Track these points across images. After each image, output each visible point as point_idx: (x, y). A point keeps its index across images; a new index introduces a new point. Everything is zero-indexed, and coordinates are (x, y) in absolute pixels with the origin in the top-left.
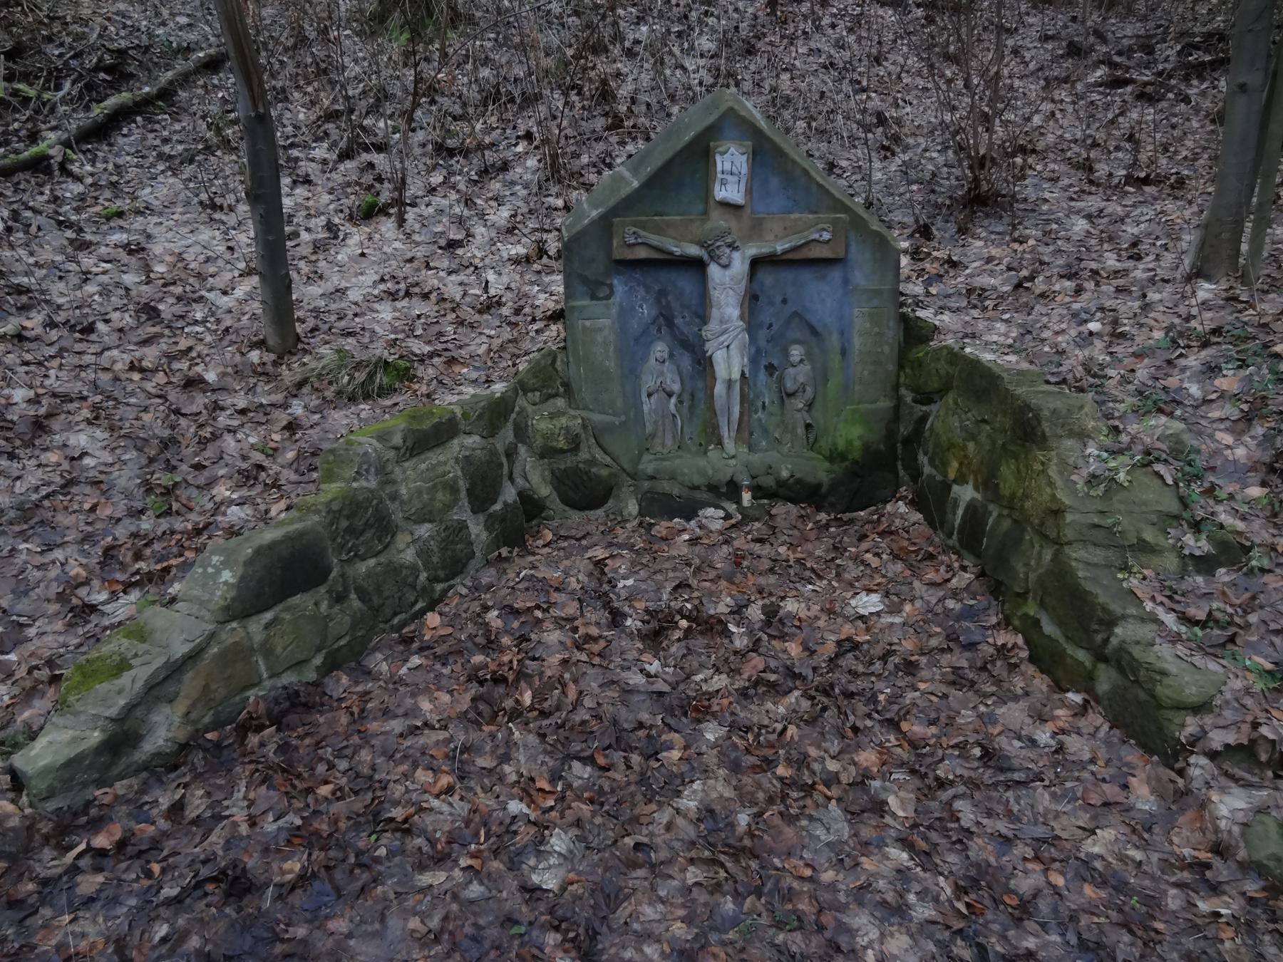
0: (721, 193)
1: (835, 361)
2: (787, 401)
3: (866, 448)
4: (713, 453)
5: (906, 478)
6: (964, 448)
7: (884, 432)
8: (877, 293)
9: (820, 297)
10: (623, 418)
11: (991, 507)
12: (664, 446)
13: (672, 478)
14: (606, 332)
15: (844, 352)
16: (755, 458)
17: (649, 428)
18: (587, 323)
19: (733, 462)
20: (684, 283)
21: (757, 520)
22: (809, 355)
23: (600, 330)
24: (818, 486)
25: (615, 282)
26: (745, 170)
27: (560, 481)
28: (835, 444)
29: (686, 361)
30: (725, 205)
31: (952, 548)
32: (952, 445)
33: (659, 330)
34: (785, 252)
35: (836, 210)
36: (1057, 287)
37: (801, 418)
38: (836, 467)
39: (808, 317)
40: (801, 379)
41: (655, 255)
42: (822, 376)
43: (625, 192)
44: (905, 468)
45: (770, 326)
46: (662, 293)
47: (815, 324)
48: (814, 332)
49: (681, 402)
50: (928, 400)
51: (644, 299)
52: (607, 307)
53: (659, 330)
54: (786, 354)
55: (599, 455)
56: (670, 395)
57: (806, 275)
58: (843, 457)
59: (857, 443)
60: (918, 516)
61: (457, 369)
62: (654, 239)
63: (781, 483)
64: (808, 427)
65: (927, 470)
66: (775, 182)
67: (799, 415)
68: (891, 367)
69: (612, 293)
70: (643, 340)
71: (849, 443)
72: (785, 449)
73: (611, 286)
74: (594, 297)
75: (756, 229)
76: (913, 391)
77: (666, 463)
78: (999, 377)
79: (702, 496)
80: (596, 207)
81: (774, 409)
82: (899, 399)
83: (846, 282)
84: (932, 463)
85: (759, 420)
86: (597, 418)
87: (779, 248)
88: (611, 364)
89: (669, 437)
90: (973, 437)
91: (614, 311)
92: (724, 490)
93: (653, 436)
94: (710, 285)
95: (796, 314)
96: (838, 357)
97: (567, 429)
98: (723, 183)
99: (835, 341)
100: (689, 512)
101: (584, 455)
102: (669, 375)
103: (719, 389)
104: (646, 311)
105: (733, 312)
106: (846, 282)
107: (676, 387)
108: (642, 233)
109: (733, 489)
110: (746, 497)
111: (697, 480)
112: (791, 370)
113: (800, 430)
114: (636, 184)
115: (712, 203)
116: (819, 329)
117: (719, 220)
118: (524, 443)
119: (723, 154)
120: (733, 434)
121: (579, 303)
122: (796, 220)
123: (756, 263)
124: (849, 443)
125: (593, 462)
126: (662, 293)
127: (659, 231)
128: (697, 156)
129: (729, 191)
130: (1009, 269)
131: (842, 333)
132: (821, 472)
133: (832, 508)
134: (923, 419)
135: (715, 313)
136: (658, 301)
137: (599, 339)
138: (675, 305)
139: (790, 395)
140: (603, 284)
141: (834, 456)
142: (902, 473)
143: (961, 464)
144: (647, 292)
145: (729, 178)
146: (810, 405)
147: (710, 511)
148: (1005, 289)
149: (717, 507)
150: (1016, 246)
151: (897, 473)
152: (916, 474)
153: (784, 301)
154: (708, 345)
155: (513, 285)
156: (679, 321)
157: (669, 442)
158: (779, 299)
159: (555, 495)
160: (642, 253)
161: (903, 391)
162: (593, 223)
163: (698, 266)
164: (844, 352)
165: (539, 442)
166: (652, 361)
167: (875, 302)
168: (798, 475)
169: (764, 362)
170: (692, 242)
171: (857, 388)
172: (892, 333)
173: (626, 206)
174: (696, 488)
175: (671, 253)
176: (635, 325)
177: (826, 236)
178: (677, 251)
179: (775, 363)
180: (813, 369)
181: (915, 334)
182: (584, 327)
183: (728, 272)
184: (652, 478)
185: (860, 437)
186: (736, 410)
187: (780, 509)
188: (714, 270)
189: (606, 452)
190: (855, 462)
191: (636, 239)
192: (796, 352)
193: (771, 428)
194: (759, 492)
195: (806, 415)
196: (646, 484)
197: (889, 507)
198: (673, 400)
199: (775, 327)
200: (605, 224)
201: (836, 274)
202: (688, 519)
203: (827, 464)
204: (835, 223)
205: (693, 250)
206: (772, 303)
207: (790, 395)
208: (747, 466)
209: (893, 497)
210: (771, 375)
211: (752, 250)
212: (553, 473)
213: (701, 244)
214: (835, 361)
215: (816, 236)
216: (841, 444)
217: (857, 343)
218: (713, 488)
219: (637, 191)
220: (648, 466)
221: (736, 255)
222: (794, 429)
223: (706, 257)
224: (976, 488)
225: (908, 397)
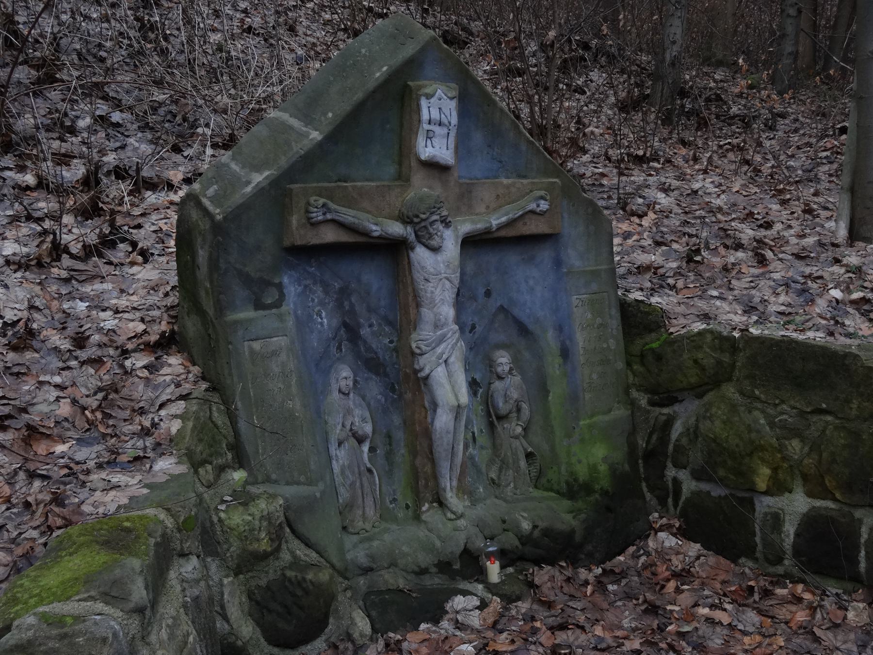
0: (426, 150)
1: (554, 365)
2: (499, 429)
3: (613, 471)
4: (430, 513)
5: (654, 502)
6: (781, 449)
7: (626, 449)
8: (595, 274)
9: (529, 285)
10: (321, 486)
11: (858, 514)
12: (364, 517)
13: (393, 564)
14: (283, 357)
15: (565, 353)
16: (480, 511)
17: (344, 494)
18: (257, 345)
19: (462, 523)
20: (371, 277)
21: (518, 599)
22: (516, 361)
23: (275, 353)
24: (573, 532)
25: (286, 280)
26: (454, 121)
27: (260, 606)
28: (572, 474)
29: (374, 389)
30: (434, 167)
31: (787, 575)
32: (756, 449)
33: (339, 348)
34: (500, 227)
35: (547, 174)
36: (732, 259)
37: (520, 447)
38: (580, 504)
39: (516, 312)
40: (515, 395)
41: (344, 237)
42: (540, 387)
43: (300, 148)
44: (651, 489)
45: (473, 327)
46: (344, 293)
47: (524, 318)
48: (523, 330)
49: (372, 449)
50: (672, 400)
51: (322, 303)
52: (281, 318)
53: (339, 348)
54: (491, 364)
55: (301, 551)
56: (360, 440)
57: (512, 257)
58: (587, 488)
59: (603, 468)
60: (694, 548)
61: (41, 448)
62: (349, 215)
63: (525, 540)
64: (529, 456)
65: (689, 485)
66: (478, 138)
67: (516, 443)
68: (620, 365)
69: (282, 296)
70: (321, 366)
71: (593, 468)
72: (509, 491)
73: (280, 287)
74: (259, 305)
75: (466, 197)
76: (646, 391)
77: (375, 543)
78: (846, 355)
79: (435, 581)
80: (258, 169)
81: (483, 440)
82: (633, 404)
83: (558, 263)
84: (697, 475)
86: (290, 491)
87: (495, 221)
88: (296, 405)
89: (369, 502)
90: (795, 433)
91: (290, 323)
92: (457, 566)
93: (350, 506)
94: (418, 276)
95: (502, 309)
96: (558, 360)
97: (268, 517)
98: (429, 135)
99: (550, 340)
100: (435, 613)
101: (286, 556)
102: (357, 412)
103: (443, 421)
104: (326, 321)
105: (448, 312)
106: (558, 263)
107: (368, 428)
108: (332, 205)
109: (470, 565)
110: (494, 570)
111: (425, 560)
112: (498, 385)
113: (523, 463)
114: (316, 136)
115: (414, 163)
116: (531, 327)
117: (421, 187)
118: (215, 554)
119: (429, 97)
120: (455, 483)
121: (242, 315)
122: (508, 187)
123: (469, 243)
124: (593, 468)
125: (296, 563)
126: (344, 293)
127: (351, 203)
128: (395, 99)
129: (436, 147)
130: (658, 244)
131: (560, 329)
132: (565, 516)
133: (591, 561)
134: (669, 422)
135: (427, 313)
136: (339, 305)
137: (276, 369)
138: (361, 309)
139: (500, 418)
140: (269, 284)
141: (574, 490)
142: (648, 496)
143: (775, 470)
144: (326, 292)
145: (437, 129)
147: (459, 602)
148: (674, 265)
149: (465, 593)
150: (636, 220)
151: (643, 497)
152: (667, 494)
153: (488, 294)
154: (422, 361)
155: (38, 303)
156: (365, 332)
157: (370, 512)
158: (482, 291)
159: (259, 634)
160: (330, 235)
161: (634, 394)
162: (260, 191)
163: (394, 250)
164: (565, 353)
165: (235, 547)
166: (336, 395)
167: (594, 287)
168: (542, 525)
170: (391, 218)
171: (588, 396)
172: (615, 323)
173: (306, 165)
174: (423, 572)
175: (366, 234)
176: (314, 342)
177: (544, 206)
178: (376, 230)
180: (523, 379)
181: (637, 321)
182: (252, 352)
183: (440, 258)
184: (367, 571)
185: (605, 459)
186: (461, 447)
187: (543, 575)
188: (420, 254)
189: (308, 545)
190: (605, 493)
191: (319, 218)
192: (503, 360)
194: (506, 557)
195: (523, 441)
196: (362, 582)
197: (651, 543)
198: (366, 448)
199: (478, 329)
200: (277, 195)
201: (545, 254)
202: (436, 621)
203: (566, 503)
204: (550, 188)
205: (396, 229)
206: (474, 298)
207: (500, 418)
208: (480, 525)
209: (651, 529)
211: (466, 227)
212: (250, 596)
213: (405, 220)
214: (554, 365)
215: (533, 206)
216: (582, 473)
217: (581, 339)
218: (444, 567)
219: (320, 145)
220: (359, 555)
221: (448, 234)
222: (516, 461)
223: (412, 238)
224: (810, 494)
225: (643, 401)
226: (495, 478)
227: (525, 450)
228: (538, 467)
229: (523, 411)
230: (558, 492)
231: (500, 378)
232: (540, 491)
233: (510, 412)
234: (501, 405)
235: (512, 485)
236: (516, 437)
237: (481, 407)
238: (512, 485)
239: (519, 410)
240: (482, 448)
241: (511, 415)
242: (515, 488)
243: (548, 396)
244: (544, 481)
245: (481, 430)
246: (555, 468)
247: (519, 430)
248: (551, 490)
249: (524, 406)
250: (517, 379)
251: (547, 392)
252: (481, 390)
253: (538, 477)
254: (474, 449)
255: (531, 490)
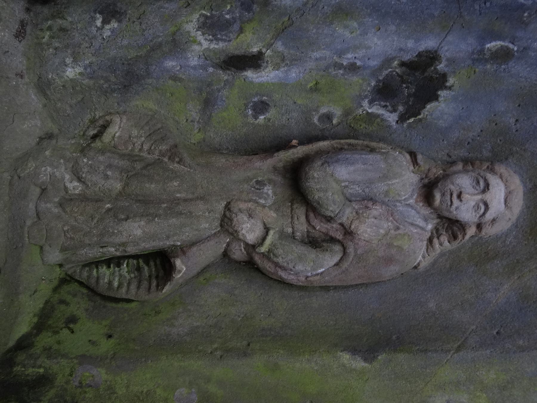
2: (263, 166)
22: (485, 254)
37: (194, 234)
40: (370, 229)
54: (482, 157)
64: (161, 262)
67: (208, 224)
81: (232, 118)
85: (177, 44)
112: (405, 180)
113: (138, 233)
146: (250, 266)
169: (453, 47)
179: (441, 109)
180: (415, 277)
193: (144, 103)
210: (385, 92)
222: (147, 207)
226: (107, 137)
227: (182, 251)
228: (123, 293)
229: (312, 254)
230: (23, 345)
231: (428, 191)
232: (45, 290)
233: (312, 208)
234: (342, 172)
235: (74, 187)
236: (226, 224)
237: (337, 112)
238: (74, 187)
239: (314, 242)
240: (208, 104)
241: (300, 211)
242: (67, 201)
243: (354, 351)
244: (78, 305)
245: (261, 107)
246: (106, 346)
247: (250, 231)
248: (41, 325)
249: (329, 260)
250: (420, 255)
251: (368, 350)
252: (392, 118)
253: (93, 292)
254: (206, 56)
255: (55, 256)
